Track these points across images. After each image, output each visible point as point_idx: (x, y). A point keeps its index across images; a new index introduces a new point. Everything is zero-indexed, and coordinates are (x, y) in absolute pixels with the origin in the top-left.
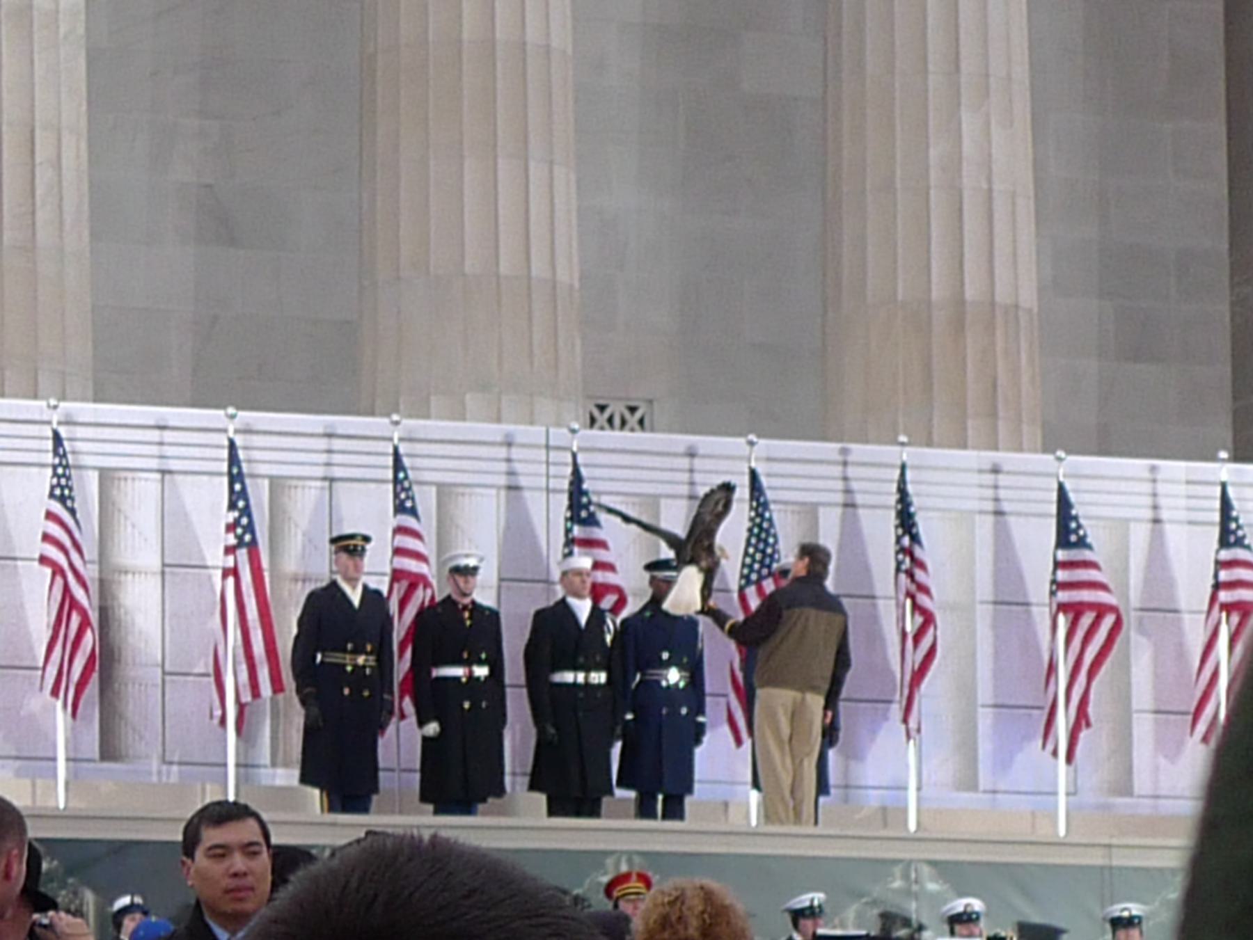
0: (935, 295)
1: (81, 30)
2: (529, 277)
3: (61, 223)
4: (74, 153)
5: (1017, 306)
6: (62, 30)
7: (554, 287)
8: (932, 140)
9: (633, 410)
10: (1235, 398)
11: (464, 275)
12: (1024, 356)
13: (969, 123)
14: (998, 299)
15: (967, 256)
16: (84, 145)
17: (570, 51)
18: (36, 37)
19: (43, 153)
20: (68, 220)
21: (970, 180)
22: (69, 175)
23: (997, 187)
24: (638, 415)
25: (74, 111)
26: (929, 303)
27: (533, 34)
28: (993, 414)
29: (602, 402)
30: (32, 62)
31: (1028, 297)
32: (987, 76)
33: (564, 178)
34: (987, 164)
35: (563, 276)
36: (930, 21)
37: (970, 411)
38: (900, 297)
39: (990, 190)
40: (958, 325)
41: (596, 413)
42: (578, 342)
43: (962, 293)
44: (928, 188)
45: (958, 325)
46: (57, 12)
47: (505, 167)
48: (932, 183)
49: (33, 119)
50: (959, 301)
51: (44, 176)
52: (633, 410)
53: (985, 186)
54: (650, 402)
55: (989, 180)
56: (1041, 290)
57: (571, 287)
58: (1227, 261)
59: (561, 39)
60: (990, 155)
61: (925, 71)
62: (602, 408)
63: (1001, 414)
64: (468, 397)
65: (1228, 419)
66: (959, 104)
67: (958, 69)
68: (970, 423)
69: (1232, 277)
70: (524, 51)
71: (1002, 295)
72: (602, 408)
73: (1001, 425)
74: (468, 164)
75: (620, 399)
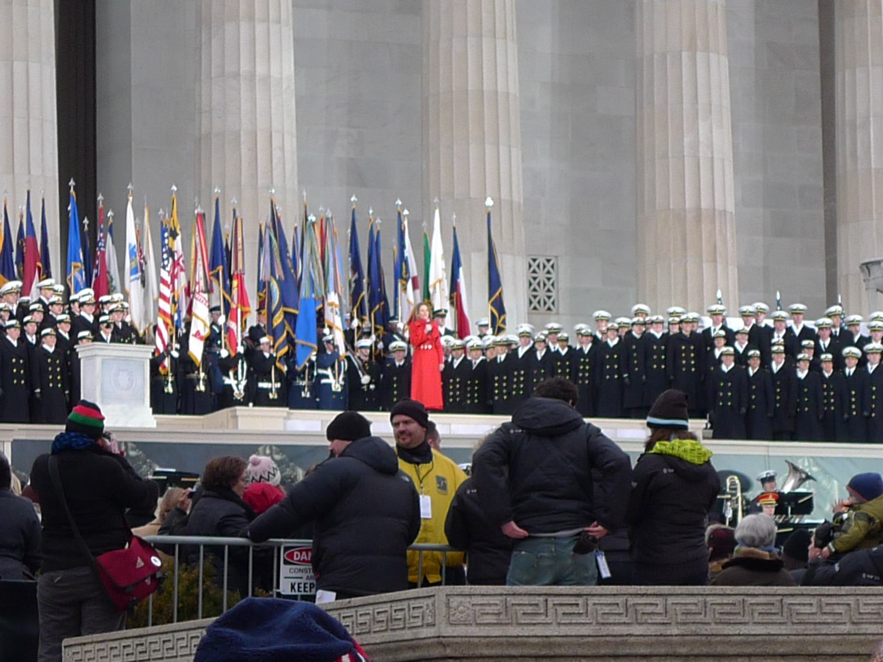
0: (687, 206)
1: (293, 87)
2: (500, 199)
3: (285, 177)
4: (291, 144)
5: (725, 211)
6: (284, 86)
7: (512, 204)
8: (685, 134)
9: (548, 261)
10: (827, 255)
11: (470, 198)
12: (728, 234)
13: (702, 125)
14: (717, 208)
15: (702, 187)
16: (294, 139)
17: (518, 95)
18: (272, 89)
19: (276, 143)
20: (287, 176)
21: (703, 152)
22: (288, 155)
23: (715, 156)
24: (551, 263)
25: (290, 124)
26: (685, 211)
27: (501, 87)
28: (715, 261)
29: (534, 257)
30: (270, 100)
31: (731, 207)
32: (710, 105)
33: (516, 153)
34: (711, 146)
35: (515, 198)
36: (684, 80)
37: (704, 259)
38: (671, 207)
39: (712, 158)
40: (698, 219)
41: (532, 262)
42: (523, 230)
43: (700, 206)
44: (684, 157)
45: (698, 219)
46: (281, 78)
47: (489, 149)
48: (685, 153)
49: (271, 127)
50: (699, 209)
51: (276, 154)
52: (548, 261)
53: (710, 155)
54: (556, 257)
55: (712, 153)
56: (736, 205)
57: (520, 204)
58: (823, 191)
59: (514, 89)
60: (712, 142)
61: (682, 102)
62: (534, 260)
63: (718, 259)
64: (473, 254)
65: (823, 264)
66: (697, 118)
67: (697, 102)
68: (704, 265)
69: (825, 198)
70: (497, 95)
71: (719, 206)
72: (534, 260)
73: (719, 267)
74: (471, 147)
75: (543, 256)
